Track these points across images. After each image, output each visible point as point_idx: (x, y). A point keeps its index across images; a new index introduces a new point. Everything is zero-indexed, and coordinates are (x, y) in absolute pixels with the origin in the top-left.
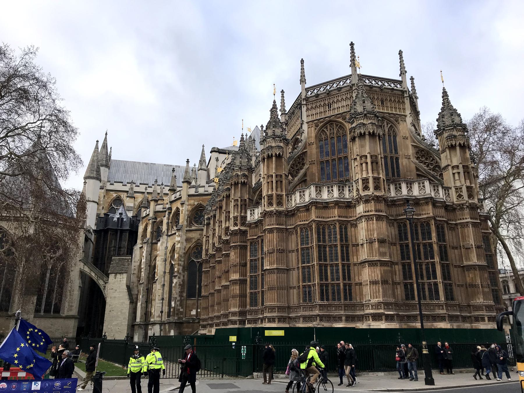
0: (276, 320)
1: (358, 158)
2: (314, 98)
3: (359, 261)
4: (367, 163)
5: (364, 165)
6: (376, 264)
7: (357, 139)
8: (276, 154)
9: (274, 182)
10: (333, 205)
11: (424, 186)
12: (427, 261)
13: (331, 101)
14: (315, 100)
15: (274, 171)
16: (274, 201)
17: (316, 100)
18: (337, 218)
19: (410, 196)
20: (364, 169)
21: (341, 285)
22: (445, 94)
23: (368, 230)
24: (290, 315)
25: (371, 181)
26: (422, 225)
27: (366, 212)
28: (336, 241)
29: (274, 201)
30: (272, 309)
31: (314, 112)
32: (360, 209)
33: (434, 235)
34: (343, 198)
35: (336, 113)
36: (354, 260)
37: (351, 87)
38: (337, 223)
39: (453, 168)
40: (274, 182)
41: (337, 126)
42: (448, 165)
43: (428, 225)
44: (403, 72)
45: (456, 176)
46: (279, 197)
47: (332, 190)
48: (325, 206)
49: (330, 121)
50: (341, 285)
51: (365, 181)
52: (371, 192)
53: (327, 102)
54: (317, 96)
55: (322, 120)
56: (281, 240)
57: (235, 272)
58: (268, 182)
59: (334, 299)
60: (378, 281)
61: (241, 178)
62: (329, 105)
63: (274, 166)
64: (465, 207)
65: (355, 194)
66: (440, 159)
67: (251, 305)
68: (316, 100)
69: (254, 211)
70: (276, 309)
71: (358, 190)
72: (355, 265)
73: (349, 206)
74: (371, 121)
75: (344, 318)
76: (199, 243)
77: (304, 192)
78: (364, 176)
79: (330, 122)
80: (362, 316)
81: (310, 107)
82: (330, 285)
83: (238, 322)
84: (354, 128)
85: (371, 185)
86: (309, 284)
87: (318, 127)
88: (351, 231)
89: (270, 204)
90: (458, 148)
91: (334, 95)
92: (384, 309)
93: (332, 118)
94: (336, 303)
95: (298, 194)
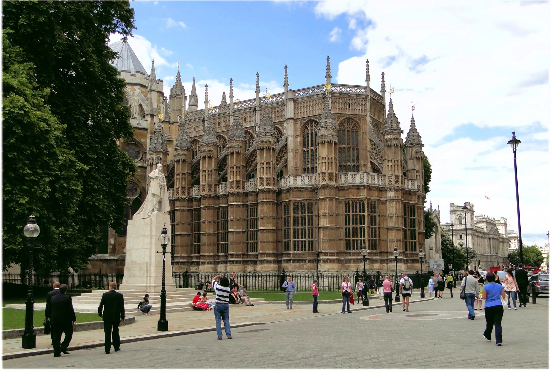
0: (336, 261)
1: (393, 160)
2: (338, 95)
3: (385, 227)
4: (398, 165)
5: (396, 166)
6: (400, 230)
7: (393, 147)
8: (335, 142)
9: (334, 163)
10: (375, 188)
11: (414, 184)
12: (412, 229)
13: (351, 103)
14: (338, 97)
15: (334, 155)
16: (334, 178)
17: (339, 97)
18: (377, 198)
19: (408, 189)
20: (396, 169)
21: (378, 240)
22: (413, 120)
23: (396, 208)
24: (341, 258)
25: (400, 178)
26: (411, 207)
27: (396, 197)
28: (375, 212)
29: (334, 178)
30: (332, 254)
31: (337, 106)
32: (391, 194)
33: (416, 214)
34: (378, 185)
35: (354, 113)
36: (382, 225)
37: (366, 97)
38: (377, 201)
39: (417, 171)
40: (334, 163)
41: (352, 123)
42: (414, 169)
43: (414, 208)
44: (383, 90)
45: (418, 177)
46: (336, 174)
47: (374, 178)
48: (369, 188)
49: (349, 118)
50: (378, 240)
51: (397, 177)
52: (399, 185)
53: (347, 102)
54: (341, 94)
55: (343, 115)
56: (336, 207)
57: (268, 223)
58: (329, 162)
59: (372, 249)
60: (401, 240)
61: (273, 145)
62: (349, 105)
63: (333, 151)
64: (421, 197)
65: (387, 184)
66: (406, 163)
67: (295, 250)
68: (339, 97)
69: (296, 177)
70: (307, 254)
71: (390, 181)
72: (382, 228)
73: (381, 190)
74: (395, 136)
75: (379, 261)
76: (132, 180)
77: (355, 175)
78: (397, 174)
79: (349, 119)
80: (387, 259)
81: (334, 101)
82: (371, 240)
83: (273, 262)
84: (391, 139)
85: (400, 180)
86: (357, 238)
87: (340, 120)
88: (381, 206)
89: (330, 179)
90: (421, 159)
91: (353, 98)
92: (403, 256)
93: (351, 116)
94: (374, 251)
95: (350, 176)
